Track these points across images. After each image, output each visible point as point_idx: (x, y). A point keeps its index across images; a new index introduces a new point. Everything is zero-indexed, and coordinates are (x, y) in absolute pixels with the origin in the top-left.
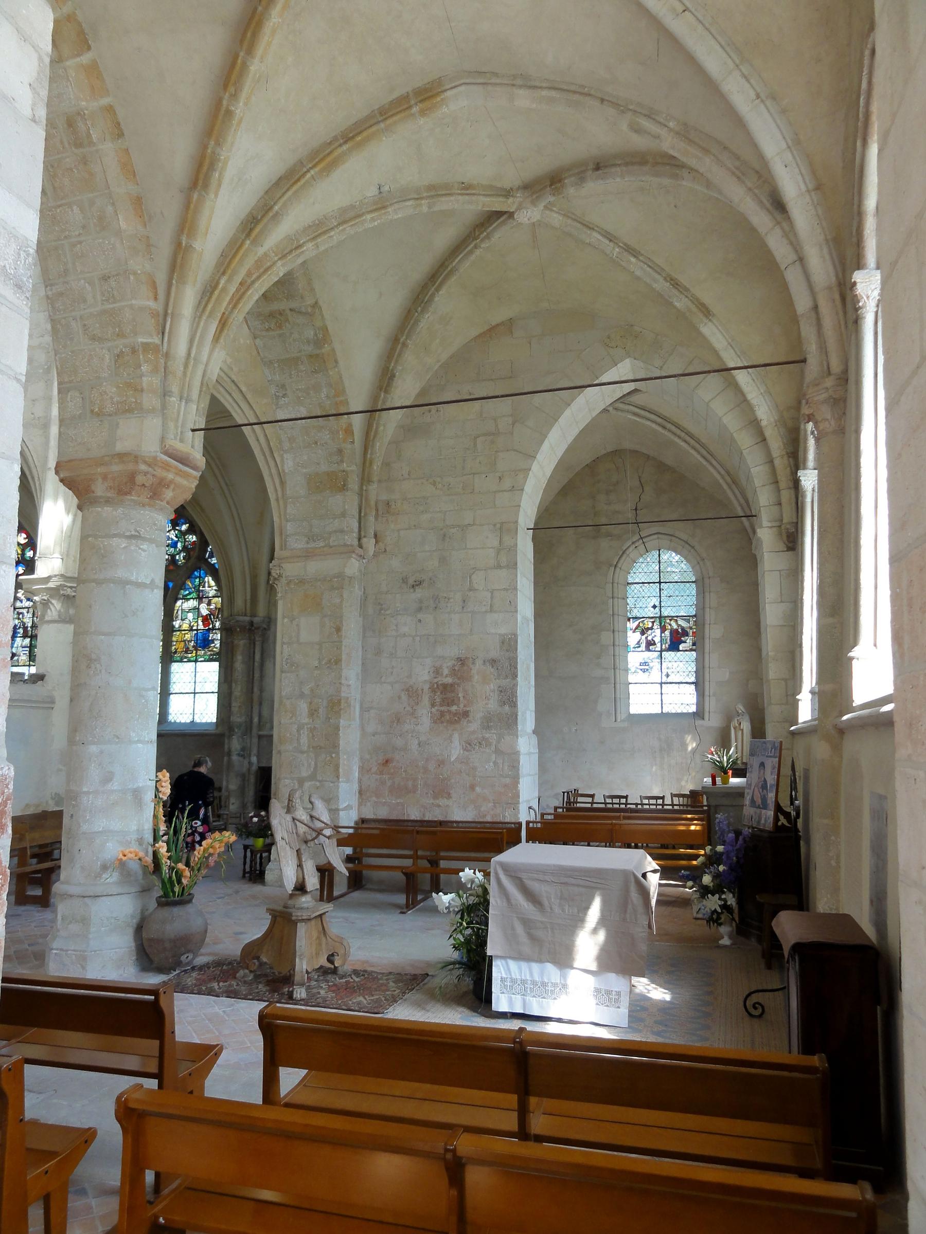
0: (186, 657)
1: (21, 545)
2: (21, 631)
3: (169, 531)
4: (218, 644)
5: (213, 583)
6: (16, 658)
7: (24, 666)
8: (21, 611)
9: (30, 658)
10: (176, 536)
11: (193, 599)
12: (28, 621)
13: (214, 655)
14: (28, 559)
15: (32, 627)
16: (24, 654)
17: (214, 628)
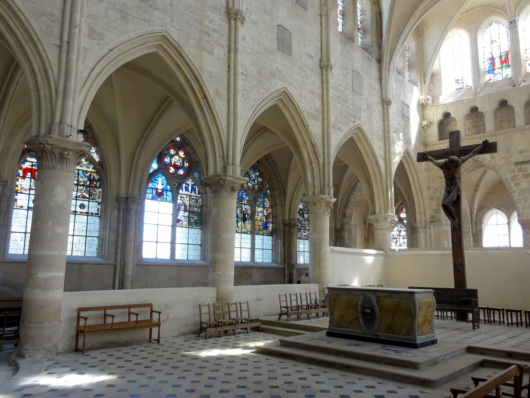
0: (259, 233)
1: (182, 158)
2: (183, 207)
3: (252, 174)
4: (271, 229)
5: (268, 202)
6: (180, 222)
7: (186, 227)
8: (183, 196)
9: (189, 224)
10: (255, 177)
11: (262, 207)
13: (269, 233)
14: (186, 167)
15: (189, 206)
16: (185, 220)
17: (269, 222)
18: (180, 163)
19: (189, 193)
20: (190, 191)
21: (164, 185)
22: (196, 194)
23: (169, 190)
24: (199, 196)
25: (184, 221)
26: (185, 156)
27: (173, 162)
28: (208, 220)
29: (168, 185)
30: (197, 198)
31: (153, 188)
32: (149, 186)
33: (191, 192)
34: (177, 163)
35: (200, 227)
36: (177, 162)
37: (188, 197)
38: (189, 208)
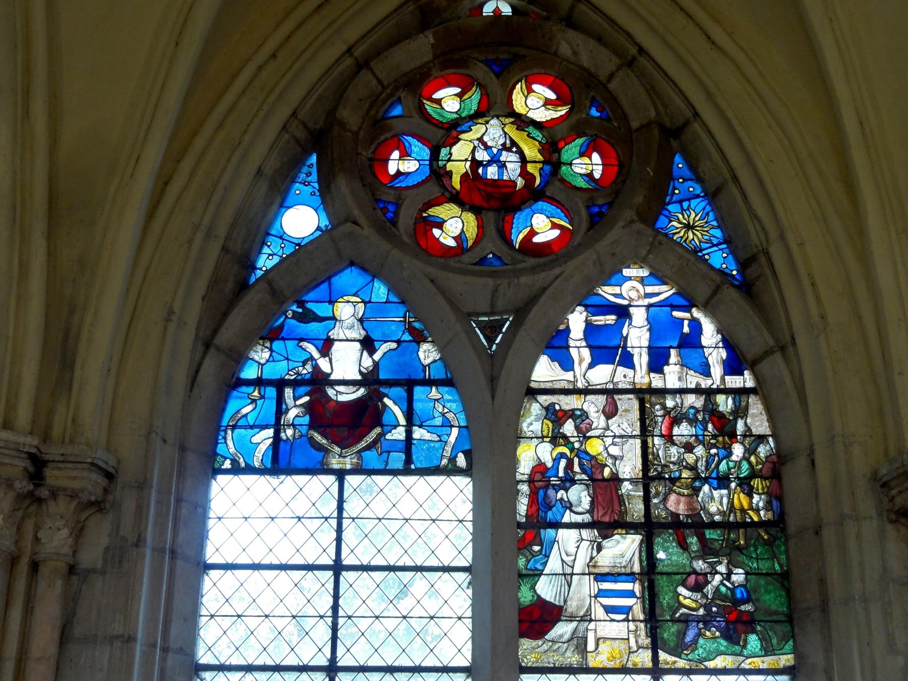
2: (580, 496)
6: (562, 629)
7: (624, 670)
12: (614, 451)
14: (581, 183)
15: (646, 480)
16: (609, 609)
18: (524, 161)
19: (641, 375)
20: (641, 359)
21: (383, 348)
22: (706, 371)
23: (438, 373)
24: (746, 380)
25: (600, 613)
26: (563, 111)
27: (458, 169)
28: (834, 574)
29: (419, 338)
30: (725, 404)
31: (280, 384)
32: (250, 372)
33: (657, 363)
34: (492, 172)
35: (786, 660)
36: (495, 160)
37: (629, 405)
38: (647, 499)
